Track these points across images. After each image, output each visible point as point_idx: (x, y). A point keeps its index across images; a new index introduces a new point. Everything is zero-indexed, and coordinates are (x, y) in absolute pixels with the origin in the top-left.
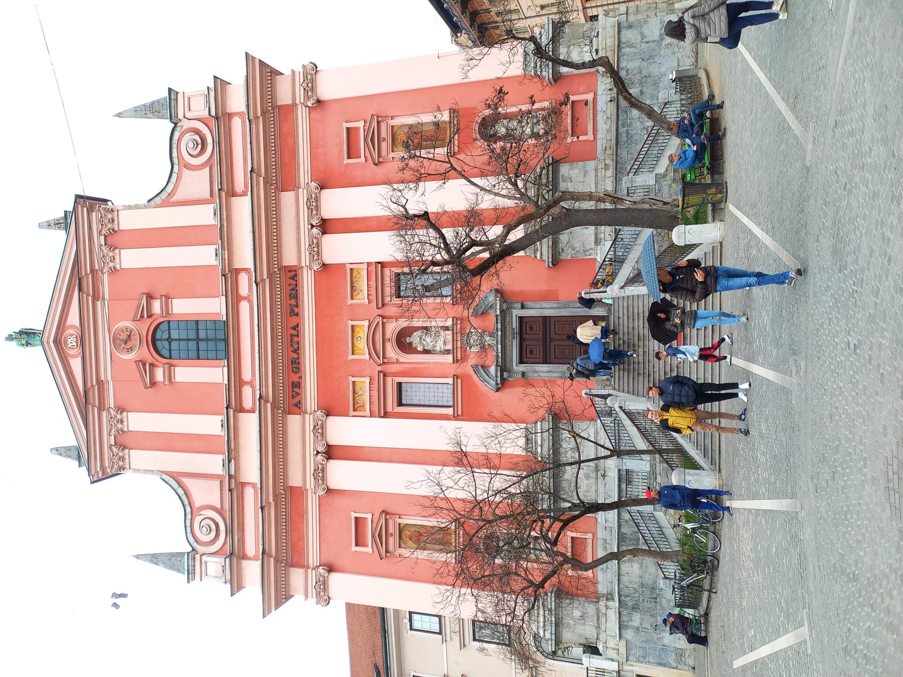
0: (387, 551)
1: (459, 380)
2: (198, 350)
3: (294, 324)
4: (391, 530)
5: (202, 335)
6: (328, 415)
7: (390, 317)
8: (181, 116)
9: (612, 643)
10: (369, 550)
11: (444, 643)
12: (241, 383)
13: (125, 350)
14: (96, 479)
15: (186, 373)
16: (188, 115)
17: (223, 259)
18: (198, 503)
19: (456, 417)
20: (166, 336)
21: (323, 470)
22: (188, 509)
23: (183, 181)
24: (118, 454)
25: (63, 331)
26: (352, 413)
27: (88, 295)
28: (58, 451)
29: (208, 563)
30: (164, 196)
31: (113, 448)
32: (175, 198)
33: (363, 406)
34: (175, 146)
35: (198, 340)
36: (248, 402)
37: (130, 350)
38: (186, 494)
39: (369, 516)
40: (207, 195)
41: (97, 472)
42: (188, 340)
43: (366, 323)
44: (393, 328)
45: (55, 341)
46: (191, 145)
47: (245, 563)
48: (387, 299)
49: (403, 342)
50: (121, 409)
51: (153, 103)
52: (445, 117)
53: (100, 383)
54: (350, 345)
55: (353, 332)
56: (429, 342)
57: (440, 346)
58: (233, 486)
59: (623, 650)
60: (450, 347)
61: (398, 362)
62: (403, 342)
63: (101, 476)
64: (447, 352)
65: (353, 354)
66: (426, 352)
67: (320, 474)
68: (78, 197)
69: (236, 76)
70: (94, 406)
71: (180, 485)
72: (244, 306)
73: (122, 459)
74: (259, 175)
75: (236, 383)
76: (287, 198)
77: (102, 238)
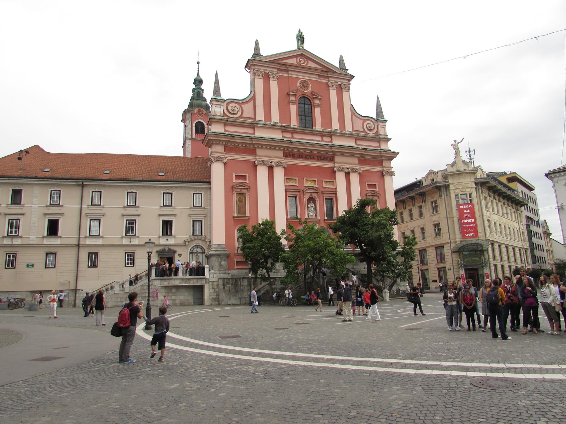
0: (235, 188)
2: (301, 115)
3: (315, 157)
4: (243, 190)
5: (307, 118)
6: (285, 168)
7: (318, 195)
8: (380, 123)
9: (215, 276)
10: (234, 181)
11: (189, 208)
12: (292, 133)
14: (250, 61)
15: (293, 109)
16: (380, 126)
17: (336, 133)
18: (243, 106)
19: (287, 219)
20: (306, 103)
21: (264, 164)
22: (241, 102)
23: (359, 120)
24: (260, 73)
25: (306, 58)
27: (321, 73)
28: (257, 44)
29: (220, 108)
30: (354, 112)
31: (263, 73)
32: (354, 116)
33: (287, 182)
34: (369, 119)
35: (305, 116)
36: (286, 135)
37: (301, 87)
38: (247, 101)
39: (247, 182)
41: (253, 63)
42: (305, 112)
43: (317, 187)
44: (315, 196)
45: (302, 54)
46: (370, 125)
47: (222, 125)
48: (324, 195)
49: (312, 200)
50: (279, 79)
51: (382, 113)
53: (287, 71)
54: (309, 179)
55: (313, 180)
58: (254, 125)
59: (214, 280)
60: (310, 217)
61: (304, 197)
63: (251, 63)
64: (308, 216)
65: (306, 180)
66: (308, 207)
67: (262, 163)
68: (353, 77)
69: (392, 146)
70: (279, 67)
71: (250, 100)
72: (320, 138)
73: (259, 76)
74: (364, 152)
75: (293, 131)
76: (356, 161)
77: (340, 83)
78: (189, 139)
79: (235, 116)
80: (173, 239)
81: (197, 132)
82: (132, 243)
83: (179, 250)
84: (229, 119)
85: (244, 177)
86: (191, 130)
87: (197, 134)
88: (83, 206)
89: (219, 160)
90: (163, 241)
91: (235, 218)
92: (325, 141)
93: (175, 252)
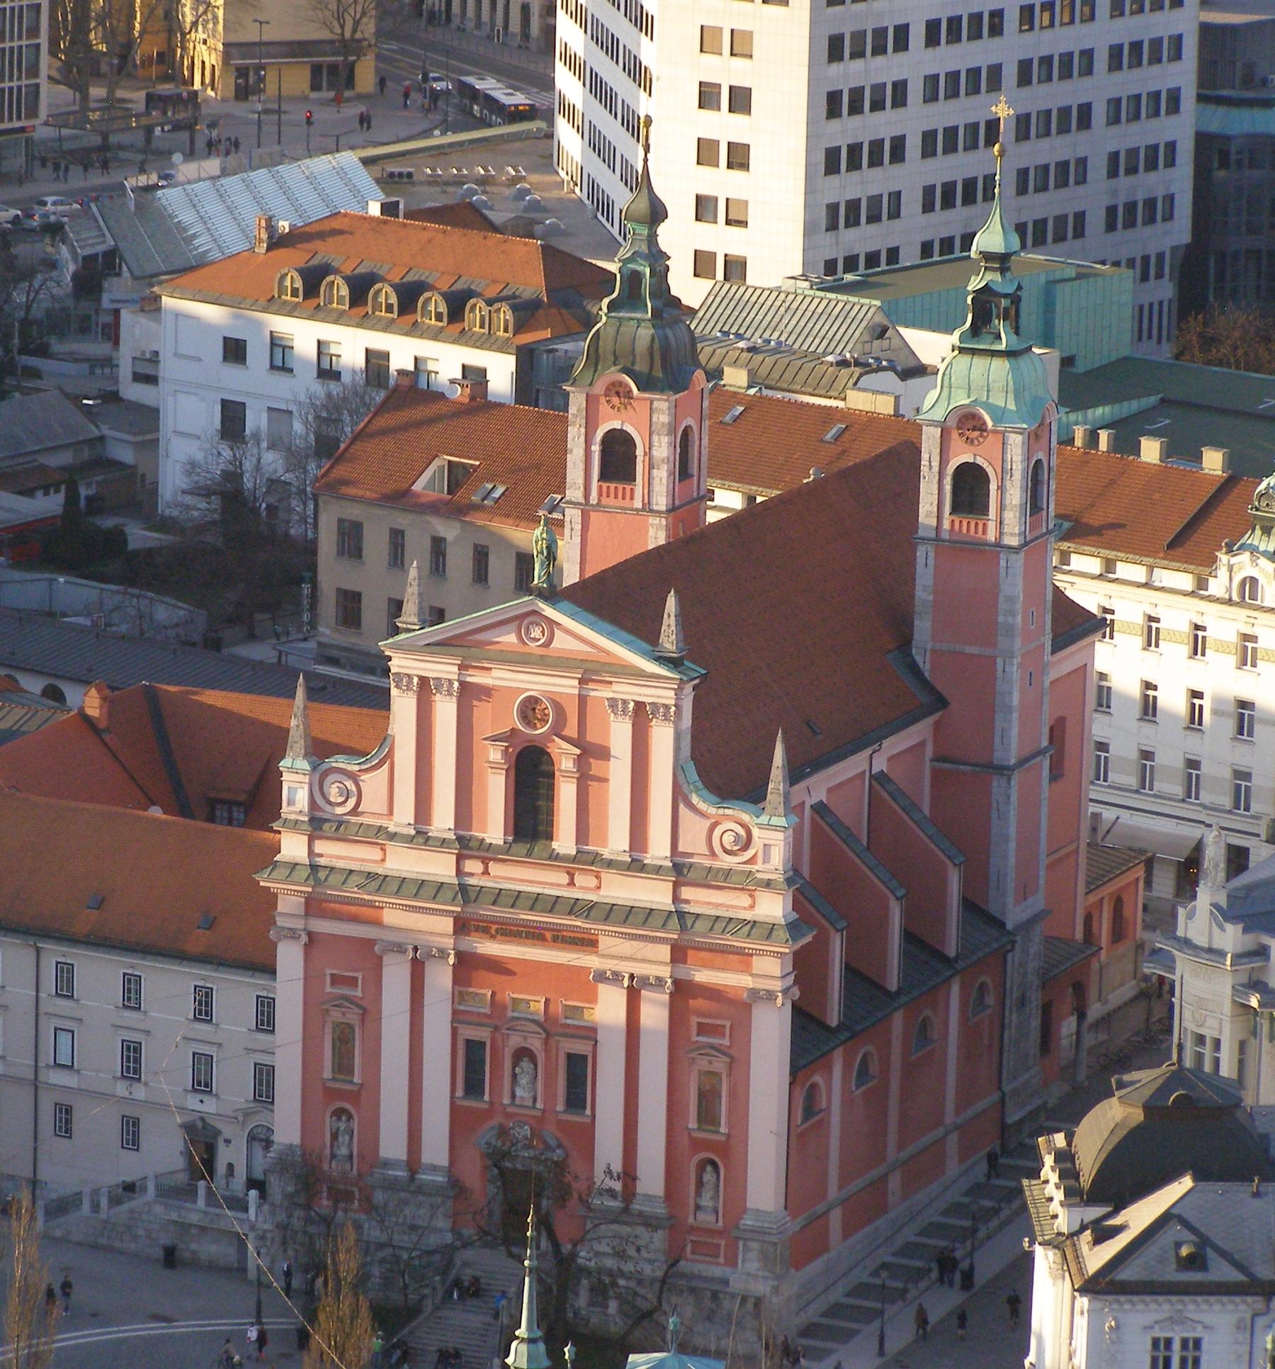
1: (485, 1106)
10: (328, 989)
13: (524, 708)
26: (457, 988)
33: (464, 1000)
39: (359, 993)
40: (680, 849)
44: (536, 1044)
46: (728, 839)
52: (723, 1129)
53: (491, 669)
56: (524, 1080)
57: (519, 1092)
62: (523, 1054)
64: (513, 1096)
66: (514, 1076)
75: (487, 854)
78: (575, 504)
79: (339, 811)
80: (214, 1100)
81: (604, 476)
82: (135, 1096)
83: (227, 1130)
84: (325, 816)
85: (353, 982)
86: (581, 466)
87: (605, 485)
88: (40, 994)
89: (292, 934)
90: (193, 1102)
91: (327, 1085)
92: (581, 888)
93: (217, 1133)
